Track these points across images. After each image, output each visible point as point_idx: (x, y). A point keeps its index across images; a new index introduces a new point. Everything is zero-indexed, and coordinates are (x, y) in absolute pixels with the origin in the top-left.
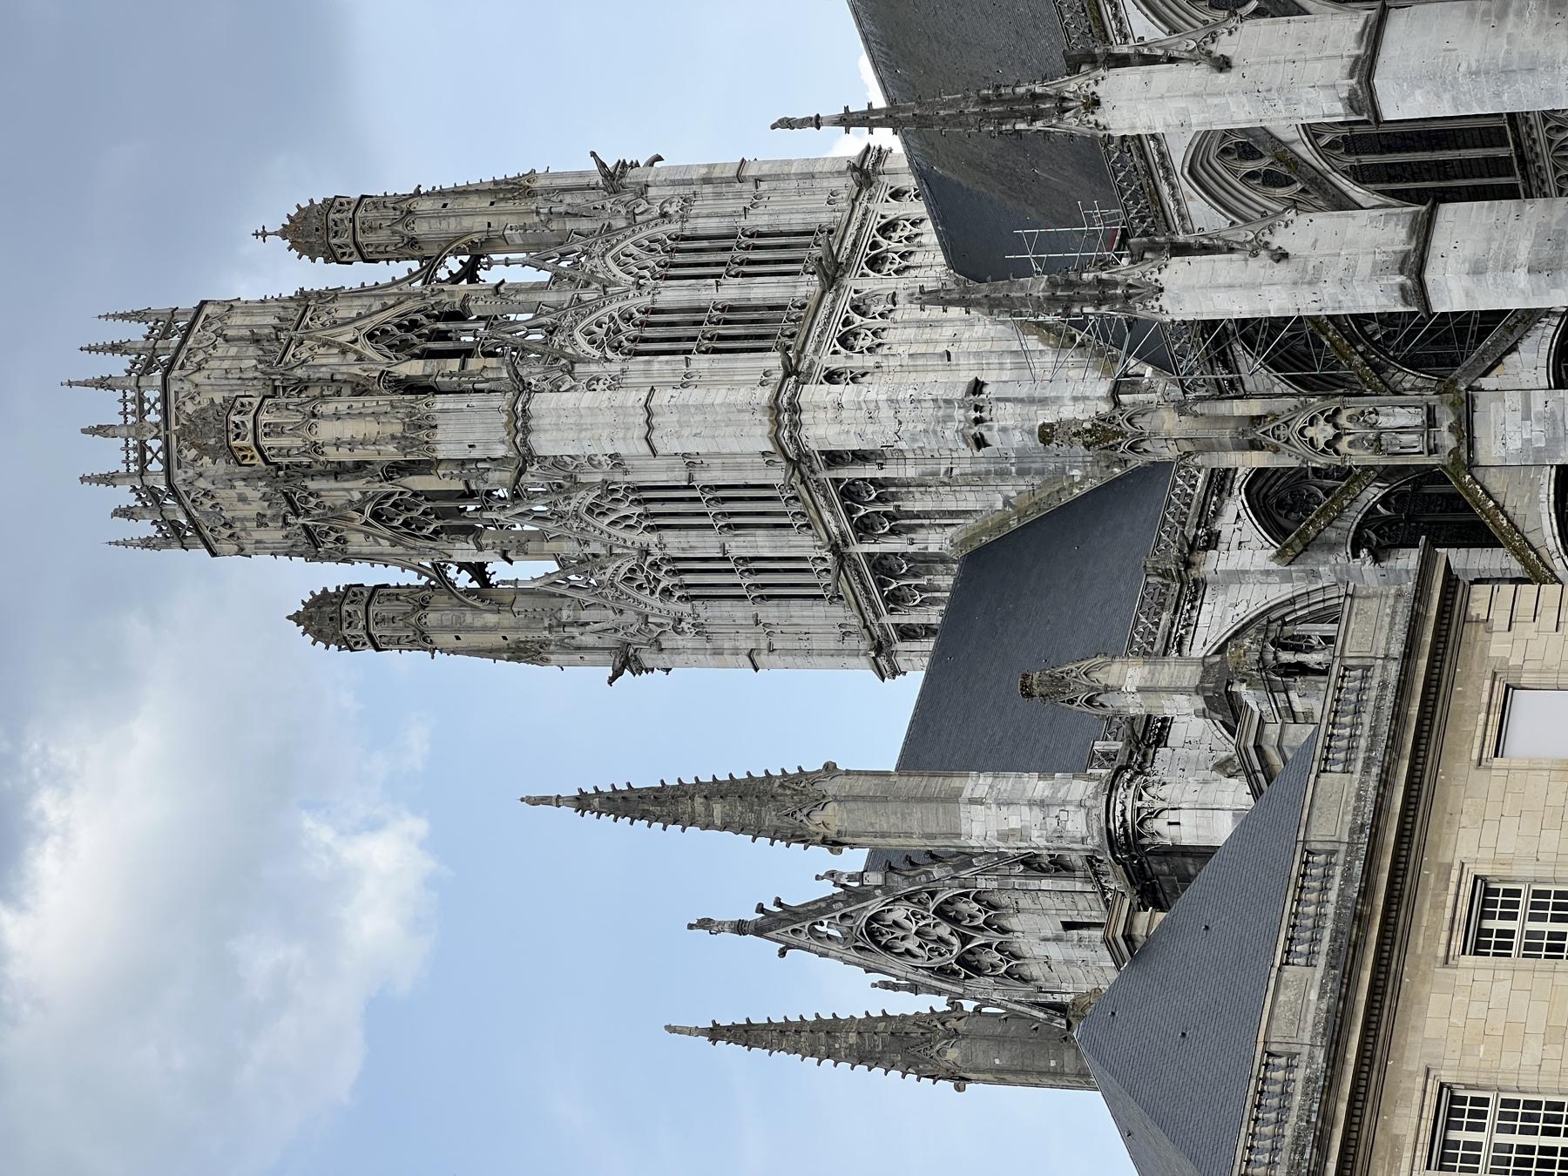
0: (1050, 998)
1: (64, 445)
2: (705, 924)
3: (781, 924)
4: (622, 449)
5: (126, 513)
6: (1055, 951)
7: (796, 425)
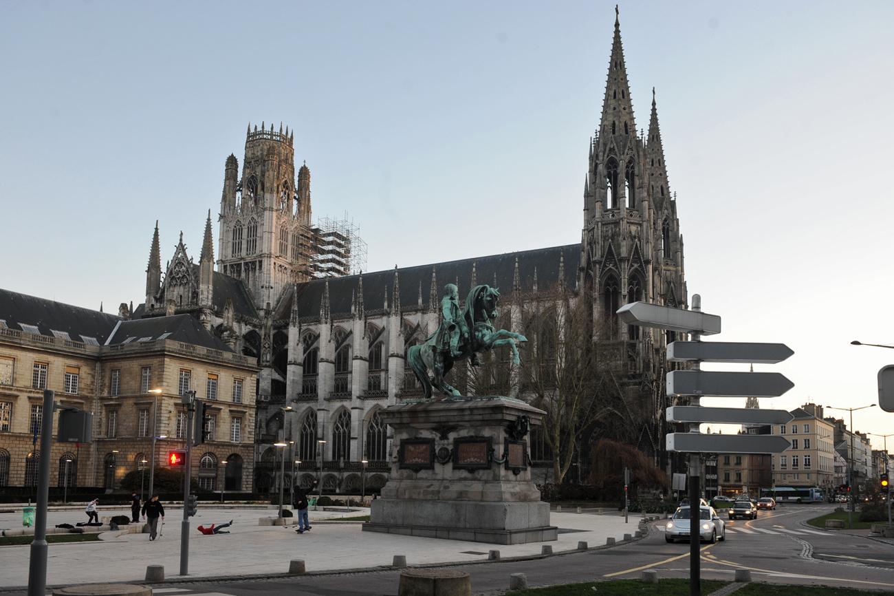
0: (166, 290)
2: (182, 234)
3: (181, 248)
4: (264, 226)
6: (175, 293)
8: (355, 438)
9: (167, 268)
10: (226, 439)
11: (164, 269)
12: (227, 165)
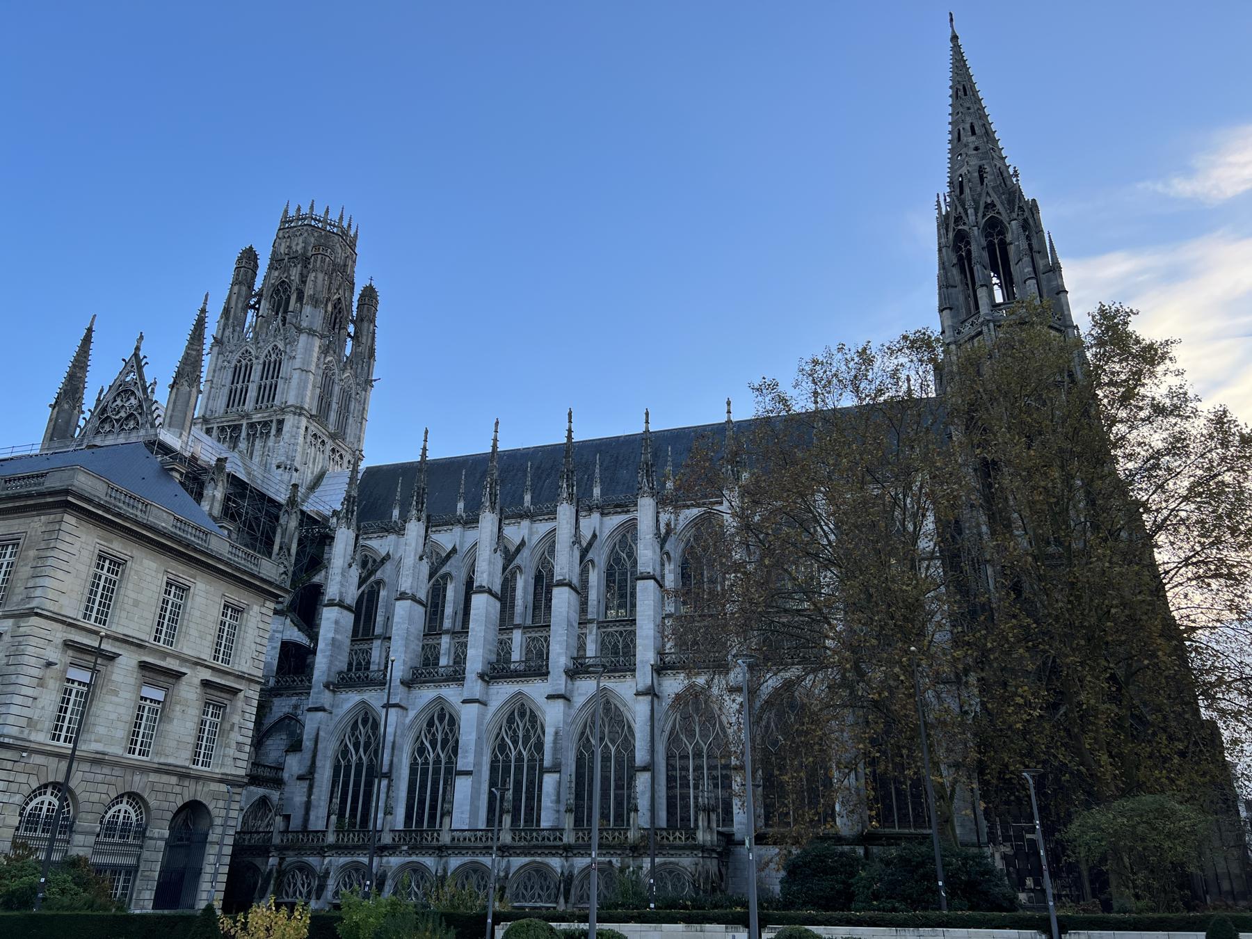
1: (328, 201)
3: (136, 363)
5: (299, 209)
7: (295, 414)
8: (469, 773)
9: (98, 399)
10: (181, 758)
11: (89, 401)
12: (240, 259)
